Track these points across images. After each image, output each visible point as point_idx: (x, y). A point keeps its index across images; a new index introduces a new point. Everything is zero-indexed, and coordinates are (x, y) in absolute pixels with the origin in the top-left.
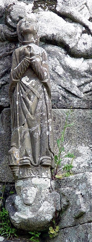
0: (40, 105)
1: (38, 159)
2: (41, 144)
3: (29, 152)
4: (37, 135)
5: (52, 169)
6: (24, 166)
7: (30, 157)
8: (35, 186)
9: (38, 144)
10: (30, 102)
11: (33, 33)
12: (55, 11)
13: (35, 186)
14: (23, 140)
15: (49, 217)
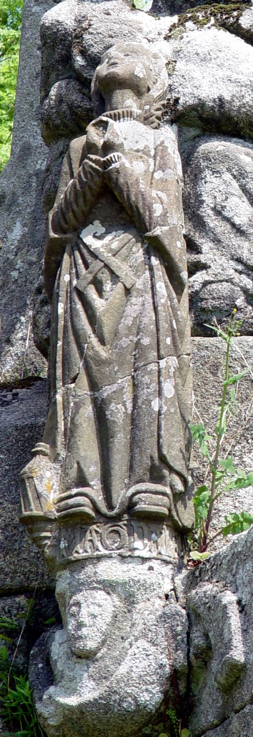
0: (132, 310)
1: (120, 495)
2: (134, 443)
3: (93, 470)
4: (119, 412)
5: (182, 534)
6: (74, 522)
7: (95, 490)
8: (109, 587)
9: (120, 441)
10: (99, 303)
11: (137, 87)
12: (236, 29)
13: (109, 587)
14: (70, 434)
15: (150, 695)
